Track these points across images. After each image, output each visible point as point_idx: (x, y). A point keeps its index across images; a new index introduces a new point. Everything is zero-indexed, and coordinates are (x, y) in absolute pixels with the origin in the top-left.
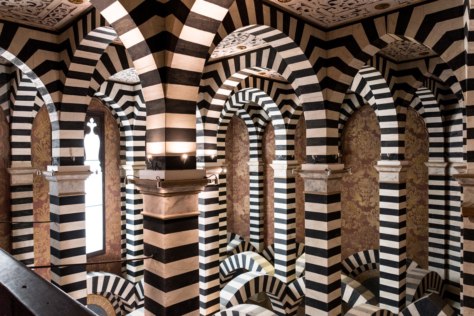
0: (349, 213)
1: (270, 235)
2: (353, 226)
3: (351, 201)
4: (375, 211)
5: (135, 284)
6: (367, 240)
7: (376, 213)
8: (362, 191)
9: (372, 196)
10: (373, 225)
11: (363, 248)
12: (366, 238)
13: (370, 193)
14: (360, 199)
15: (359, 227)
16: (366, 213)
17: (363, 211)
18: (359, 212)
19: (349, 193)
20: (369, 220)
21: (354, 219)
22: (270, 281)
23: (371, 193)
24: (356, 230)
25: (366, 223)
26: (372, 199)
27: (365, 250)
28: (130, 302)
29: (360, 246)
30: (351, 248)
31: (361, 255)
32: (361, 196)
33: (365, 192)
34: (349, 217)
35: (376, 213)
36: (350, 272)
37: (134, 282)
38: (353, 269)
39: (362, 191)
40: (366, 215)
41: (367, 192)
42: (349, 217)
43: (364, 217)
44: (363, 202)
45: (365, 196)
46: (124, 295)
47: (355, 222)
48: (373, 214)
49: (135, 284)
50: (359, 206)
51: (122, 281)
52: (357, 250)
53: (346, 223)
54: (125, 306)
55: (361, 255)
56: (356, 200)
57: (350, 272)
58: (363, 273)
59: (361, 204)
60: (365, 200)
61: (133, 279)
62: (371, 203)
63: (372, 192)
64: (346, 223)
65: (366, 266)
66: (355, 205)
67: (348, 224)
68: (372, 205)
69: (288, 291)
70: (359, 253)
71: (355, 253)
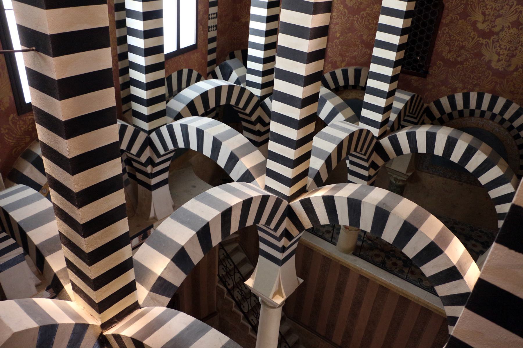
0: (458, 38)
1: (330, 57)
2: (458, 57)
3: (465, 19)
4: (496, 39)
5: (150, 132)
6: (473, 78)
7: (498, 41)
8: (488, 7)
9: (500, 16)
10: (487, 59)
11: (464, 88)
12: (472, 76)
13: (499, 11)
14: (480, 18)
15: (466, 60)
16: (482, 41)
17: (479, 37)
18: (473, 39)
19: (465, 8)
20: (484, 51)
21: (463, 47)
22: (364, 134)
23: (501, 11)
24: (462, 63)
25: (479, 55)
26: (499, 21)
27: (465, 91)
28: (143, 159)
29: (461, 85)
30: (446, 87)
31: (459, 98)
32: (484, 14)
33: (492, 9)
34: (456, 44)
35: (498, 41)
36: (437, 117)
37: (147, 129)
38: (442, 115)
39: (488, 7)
40: (482, 44)
41: (495, 9)
42: (456, 44)
43: (478, 45)
44: (483, 23)
45: (489, 14)
46: (135, 150)
47: (463, 51)
48: (493, 42)
49: (150, 132)
50: (475, 29)
51: (130, 130)
52: (455, 91)
53: (450, 51)
54: (133, 162)
55: (459, 98)
56: (473, 19)
57: (437, 117)
58: (454, 121)
59: (480, 26)
60: (488, 20)
61: (145, 125)
62: (496, 26)
63: (502, 8)
64: (450, 51)
65: (461, 113)
66: (469, 27)
67: (452, 54)
68: (496, 30)
69: (379, 149)
70: (456, 95)
71: (450, 94)
